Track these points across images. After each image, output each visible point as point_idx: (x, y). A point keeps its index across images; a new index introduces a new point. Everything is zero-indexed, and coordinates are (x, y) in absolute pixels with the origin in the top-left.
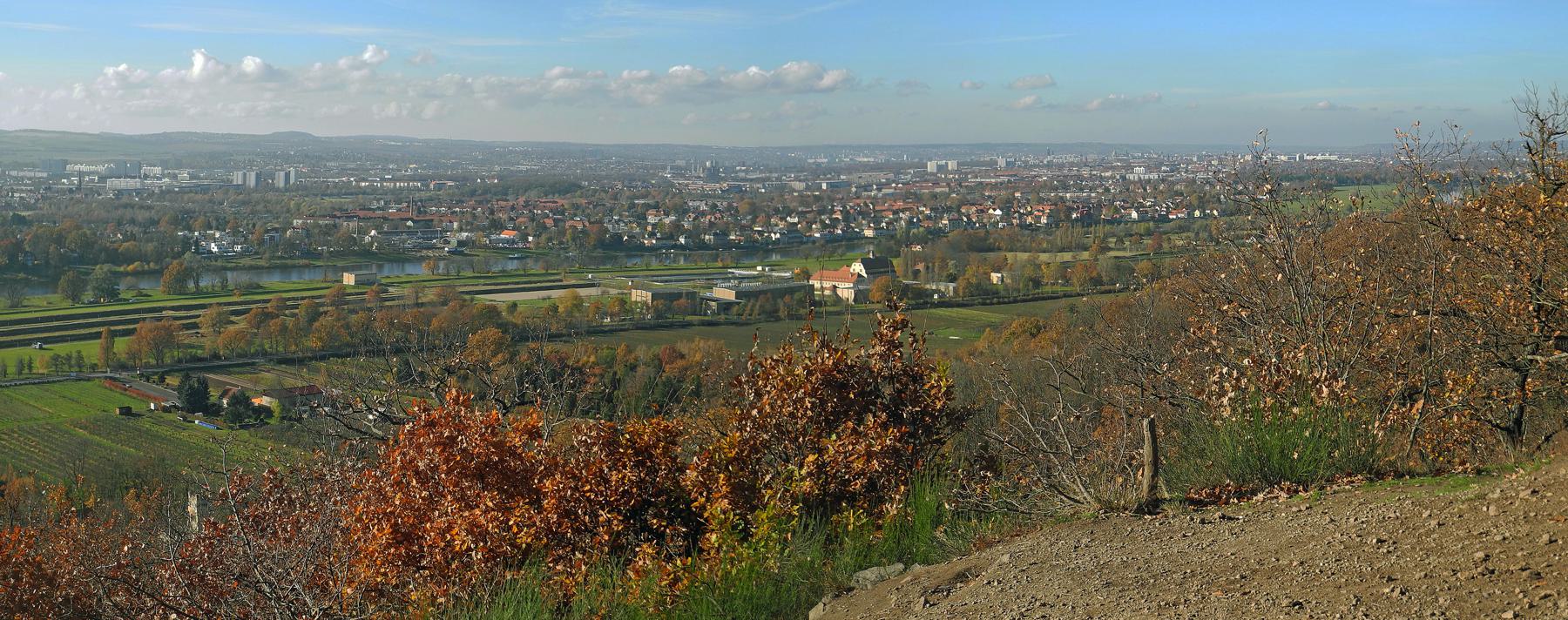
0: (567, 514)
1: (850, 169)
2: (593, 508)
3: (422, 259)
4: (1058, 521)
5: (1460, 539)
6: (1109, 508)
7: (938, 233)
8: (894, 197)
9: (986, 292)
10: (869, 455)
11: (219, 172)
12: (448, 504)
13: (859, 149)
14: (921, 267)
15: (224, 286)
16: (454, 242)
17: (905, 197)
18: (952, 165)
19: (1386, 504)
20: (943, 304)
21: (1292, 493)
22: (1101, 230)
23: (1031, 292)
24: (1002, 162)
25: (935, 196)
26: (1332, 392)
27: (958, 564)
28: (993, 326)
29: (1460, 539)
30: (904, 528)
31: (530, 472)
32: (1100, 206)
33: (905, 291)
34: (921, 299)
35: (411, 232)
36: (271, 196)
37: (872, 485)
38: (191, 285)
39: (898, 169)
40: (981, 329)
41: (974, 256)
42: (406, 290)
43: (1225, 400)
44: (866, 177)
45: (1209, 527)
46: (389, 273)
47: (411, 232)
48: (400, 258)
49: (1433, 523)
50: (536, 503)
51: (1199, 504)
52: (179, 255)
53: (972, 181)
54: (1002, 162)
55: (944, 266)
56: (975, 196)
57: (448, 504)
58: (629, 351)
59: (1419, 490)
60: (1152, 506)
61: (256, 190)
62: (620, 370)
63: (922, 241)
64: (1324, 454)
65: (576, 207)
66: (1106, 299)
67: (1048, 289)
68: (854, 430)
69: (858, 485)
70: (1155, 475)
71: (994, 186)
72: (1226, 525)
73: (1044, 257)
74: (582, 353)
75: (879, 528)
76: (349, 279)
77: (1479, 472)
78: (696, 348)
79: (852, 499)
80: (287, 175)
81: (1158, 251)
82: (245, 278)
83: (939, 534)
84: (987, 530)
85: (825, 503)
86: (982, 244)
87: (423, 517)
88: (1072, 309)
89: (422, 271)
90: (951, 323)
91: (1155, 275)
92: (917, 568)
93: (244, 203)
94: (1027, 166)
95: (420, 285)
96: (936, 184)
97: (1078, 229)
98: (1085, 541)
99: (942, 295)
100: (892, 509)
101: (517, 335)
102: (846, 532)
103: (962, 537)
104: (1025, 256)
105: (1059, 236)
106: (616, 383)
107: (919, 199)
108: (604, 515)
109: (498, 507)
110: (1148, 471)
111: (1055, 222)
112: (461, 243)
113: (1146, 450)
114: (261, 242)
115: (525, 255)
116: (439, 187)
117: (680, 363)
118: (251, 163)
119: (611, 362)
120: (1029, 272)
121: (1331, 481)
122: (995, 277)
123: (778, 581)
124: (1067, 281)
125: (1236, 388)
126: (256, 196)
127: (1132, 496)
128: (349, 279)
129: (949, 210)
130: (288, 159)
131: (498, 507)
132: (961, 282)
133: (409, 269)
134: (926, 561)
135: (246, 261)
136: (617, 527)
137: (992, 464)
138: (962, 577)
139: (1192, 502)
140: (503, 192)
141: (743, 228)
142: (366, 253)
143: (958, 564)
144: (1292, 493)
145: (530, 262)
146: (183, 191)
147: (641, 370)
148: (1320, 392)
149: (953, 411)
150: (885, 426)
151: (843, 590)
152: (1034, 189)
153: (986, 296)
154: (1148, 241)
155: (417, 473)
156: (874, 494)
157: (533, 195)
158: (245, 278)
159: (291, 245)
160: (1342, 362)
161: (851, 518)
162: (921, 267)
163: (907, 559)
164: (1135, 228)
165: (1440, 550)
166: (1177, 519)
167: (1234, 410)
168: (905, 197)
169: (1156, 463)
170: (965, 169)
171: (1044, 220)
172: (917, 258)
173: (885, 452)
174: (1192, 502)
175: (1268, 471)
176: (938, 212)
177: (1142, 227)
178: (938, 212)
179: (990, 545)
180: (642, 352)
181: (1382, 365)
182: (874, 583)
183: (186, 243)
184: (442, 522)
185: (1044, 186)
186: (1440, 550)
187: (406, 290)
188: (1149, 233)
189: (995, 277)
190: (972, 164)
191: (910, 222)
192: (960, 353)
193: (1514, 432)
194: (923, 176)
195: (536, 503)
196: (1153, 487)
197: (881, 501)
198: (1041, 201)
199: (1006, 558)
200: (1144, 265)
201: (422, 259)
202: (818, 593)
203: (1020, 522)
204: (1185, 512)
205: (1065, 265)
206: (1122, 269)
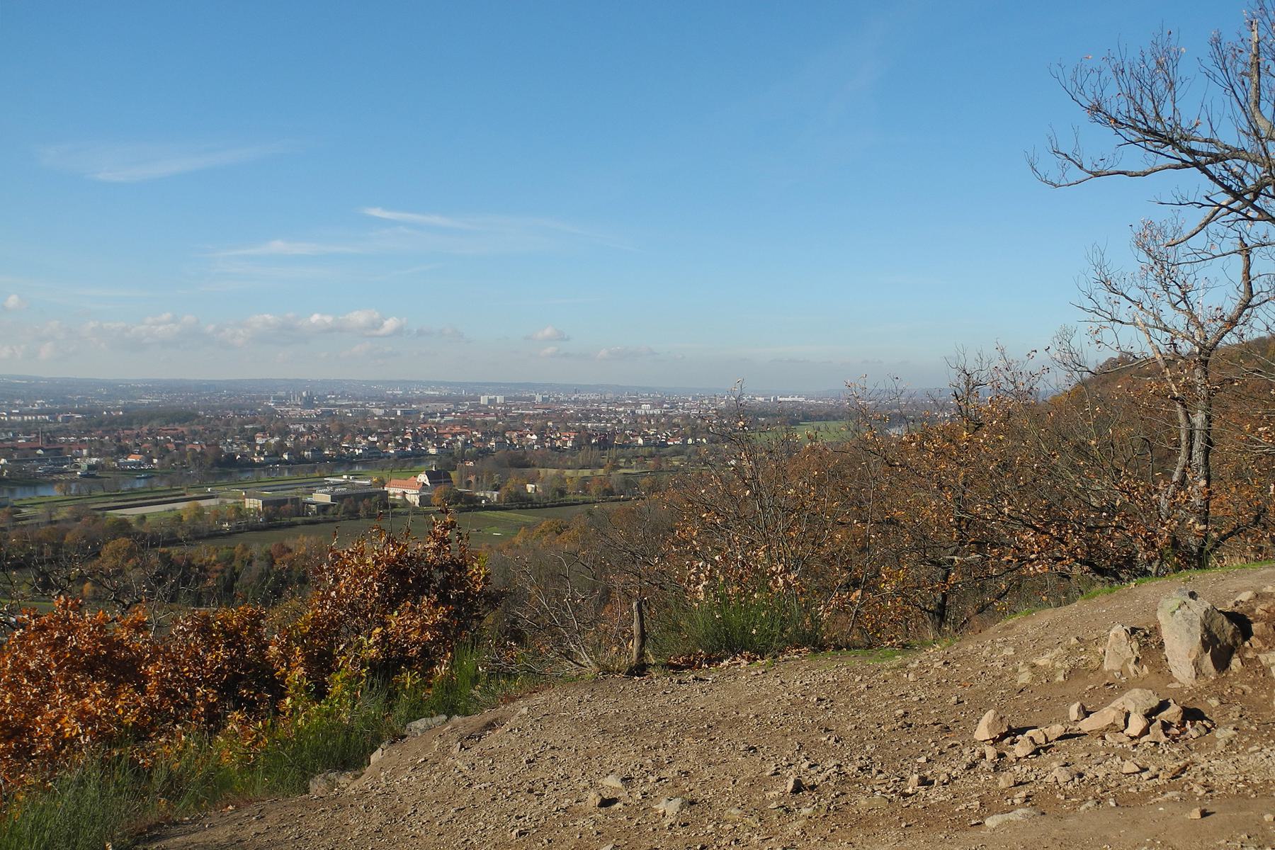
0: (166, 693)
1: (420, 400)
2: (191, 685)
4: (566, 681)
5: (884, 699)
6: (607, 671)
7: (486, 452)
8: (453, 423)
9: (522, 499)
10: (424, 628)
12: (59, 696)
13: (428, 384)
14: (472, 478)
17: (462, 423)
18: (500, 399)
19: (826, 670)
20: (490, 507)
21: (752, 660)
22: (614, 453)
23: (558, 499)
24: (539, 398)
25: (485, 423)
26: (786, 582)
27: (488, 715)
28: (528, 526)
29: (884, 699)
30: (449, 686)
31: (140, 659)
32: (614, 433)
34: (472, 504)
37: (425, 652)
39: (458, 401)
40: (518, 528)
41: (514, 470)
43: (700, 587)
45: (685, 686)
49: (863, 686)
50: (141, 689)
51: (677, 668)
53: (515, 412)
54: (539, 398)
55: (490, 478)
56: (516, 424)
57: (59, 696)
58: (246, 549)
59: (854, 660)
60: (640, 669)
62: (237, 564)
63: (474, 458)
64: (777, 630)
65: (195, 433)
66: (616, 505)
67: (571, 497)
68: (412, 609)
69: (414, 652)
70: (642, 646)
71: (532, 417)
72: (697, 685)
73: (568, 473)
74: (205, 553)
75: (430, 686)
77: (904, 646)
78: (301, 543)
79: (410, 663)
81: (658, 470)
83: (476, 693)
84: (513, 688)
85: (386, 669)
86: (520, 462)
87: (33, 710)
88: (590, 513)
90: (495, 523)
91: (653, 489)
92: (456, 719)
94: (559, 402)
96: (487, 414)
97: (596, 451)
98: (587, 696)
99: (488, 501)
100: (441, 670)
101: (146, 541)
102: (404, 689)
103: (493, 693)
104: (554, 471)
105: (581, 457)
106: (235, 576)
107: (473, 425)
108: (200, 691)
109: (107, 694)
110: (636, 642)
111: (578, 445)
113: (635, 626)
115: (150, 475)
117: (288, 556)
119: (231, 558)
120: (556, 484)
121: (782, 652)
122: (530, 487)
123: (349, 731)
124: (586, 491)
125: (709, 578)
127: (624, 661)
129: (496, 434)
131: (107, 694)
132: (503, 491)
134: (466, 714)
136: (212, 699)
137: (518, 637)
138: (491, 726)
139: (672, 666)
143: (488, 715)
144: (752, 660)
145: (156, 481)
147: (256, 564)
148: (776, 582)
149: (490, 594)
150: (436, 605)
151: (398, 737)
152: (562, 420)
153: (521, 502)
154: (650, 462)
155: (28, 672)
156: (427, 659)
160: (799, 560)
161: (408, 679)
162: (472, 478)
163: (451, 710)
164: (641, 452)
165: (868, 707)
166: (660, 680)
167: (707, 594)
168: (462, 423)
169: (643, 636)
170: (510, 403)
171: (569, 444)
172: (469, 471)
173: (436, 626)
174: (672, 666)
175: (730, 642)
176: (488, 435)
177: (646, 451)
178: (488, 435)
179: (513, 700)
180: (256, 550)
181: (830, 561)
182: (423, 731)
184: (53, 714)
185: (571, 417)
186: (868, 707)
188: (651, 456)
189: (530, 487)
190: (516, 399)
191: (465, 443)
192: (498, 548)
193: (940, 614)
194: (477, 407)
195: (141, 689)
196: (641, 655)
197: (433, 664)
198: (568, 429)
199: (525, 711)
200: (646, 481)
202: (378, 740)
203: (538, 680)
204: (666, 675)
205: (585, 479)
206: (628, 482)
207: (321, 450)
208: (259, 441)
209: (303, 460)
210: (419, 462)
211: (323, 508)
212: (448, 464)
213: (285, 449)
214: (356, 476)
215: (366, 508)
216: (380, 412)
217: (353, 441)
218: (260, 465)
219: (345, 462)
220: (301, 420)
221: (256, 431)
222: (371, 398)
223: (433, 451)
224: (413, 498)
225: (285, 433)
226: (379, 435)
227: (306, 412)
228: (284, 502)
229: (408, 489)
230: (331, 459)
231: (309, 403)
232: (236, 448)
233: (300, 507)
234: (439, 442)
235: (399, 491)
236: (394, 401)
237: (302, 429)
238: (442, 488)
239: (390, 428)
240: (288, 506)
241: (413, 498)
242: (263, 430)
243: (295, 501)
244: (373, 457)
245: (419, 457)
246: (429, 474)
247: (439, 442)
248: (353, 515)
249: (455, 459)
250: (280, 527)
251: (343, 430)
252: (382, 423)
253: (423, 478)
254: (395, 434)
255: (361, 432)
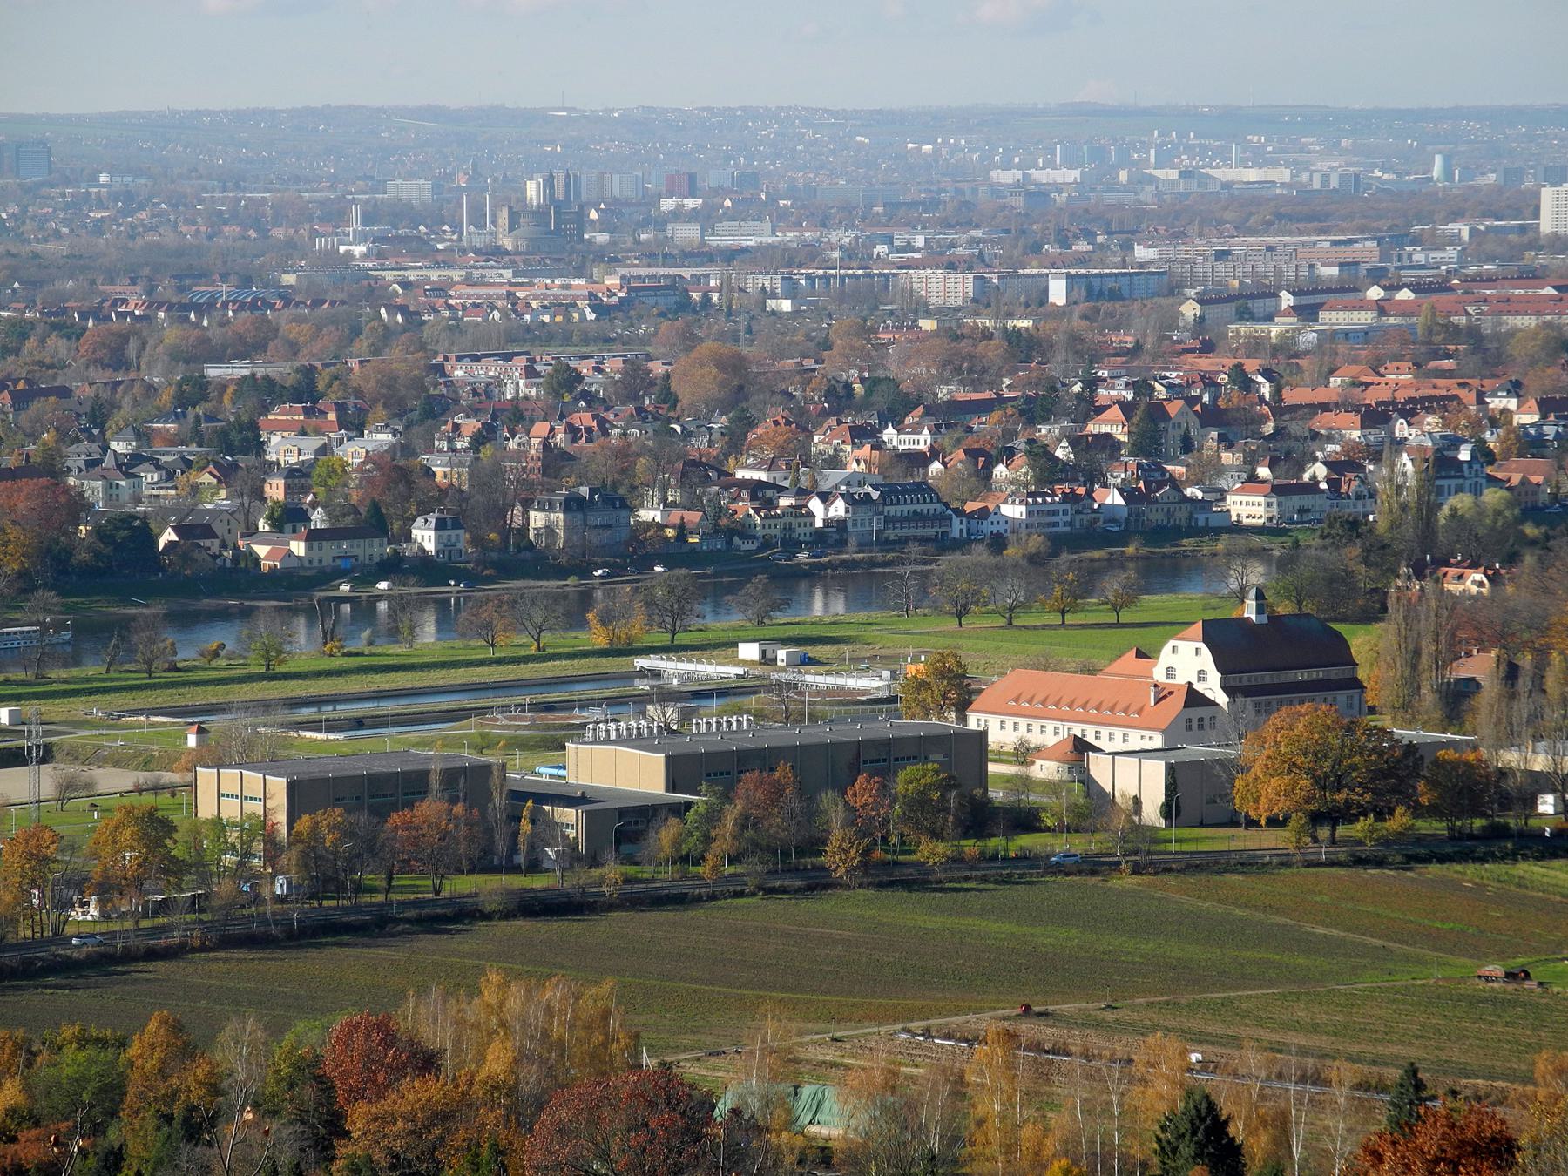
8: (1374, 348)
13: (1230, 126)
14: (1480, 666)
17: (1425, 349)
33: (1398, 773)
39: (1402, 219)
44: (1249, 255)
63: (1495, 548)
107: (1489, 356)
141: (697, 472)
162: (1480, 666)
168: (1425, 349)
172: (1464, 627)
191: (1441, 464)
207: (617, 501)
208: (283, 448)
209: (520, 559)
210: (1164, 571)
211: (625, 825)
212: (1338, 585)
213: (432, 499)
214: (811, 646)
215: (865, 829)
216: (947, 288)
217: (796, 455)
218: (291, 585)
219: (750, 566)
220: (516, 339)
221: (267, 393)
222: (901, 213)
223: (1248, 507)
224: (1136, 778)
225: (423, 407)
226: (947, 416)
227: (538, 293)
228: (411, 785)
229: (1104, 722)
230: (676, 552)
231: (557, 237)
232: (152, 487)
233: (496, 819)
234: (1287, 454)
235: (1049, 734)
236: (1034, 227)
237: (517, 386)
238: (1300, 721)
239: (1015, 380)
240: (430, 808)
241: (1136, 778)
242: (305, 393)
243: (469, 782)
244: (906, 545)
245: (1166, 543)
246: (1227, 642)
247: (1287, 454)
248: (794, 865)
249: (1380, 553)
250: (377, 926)
251: (740, 393)
252: (958, 349)
253: (1188, 662)
254: (1034, 410)
255: (839, 398)
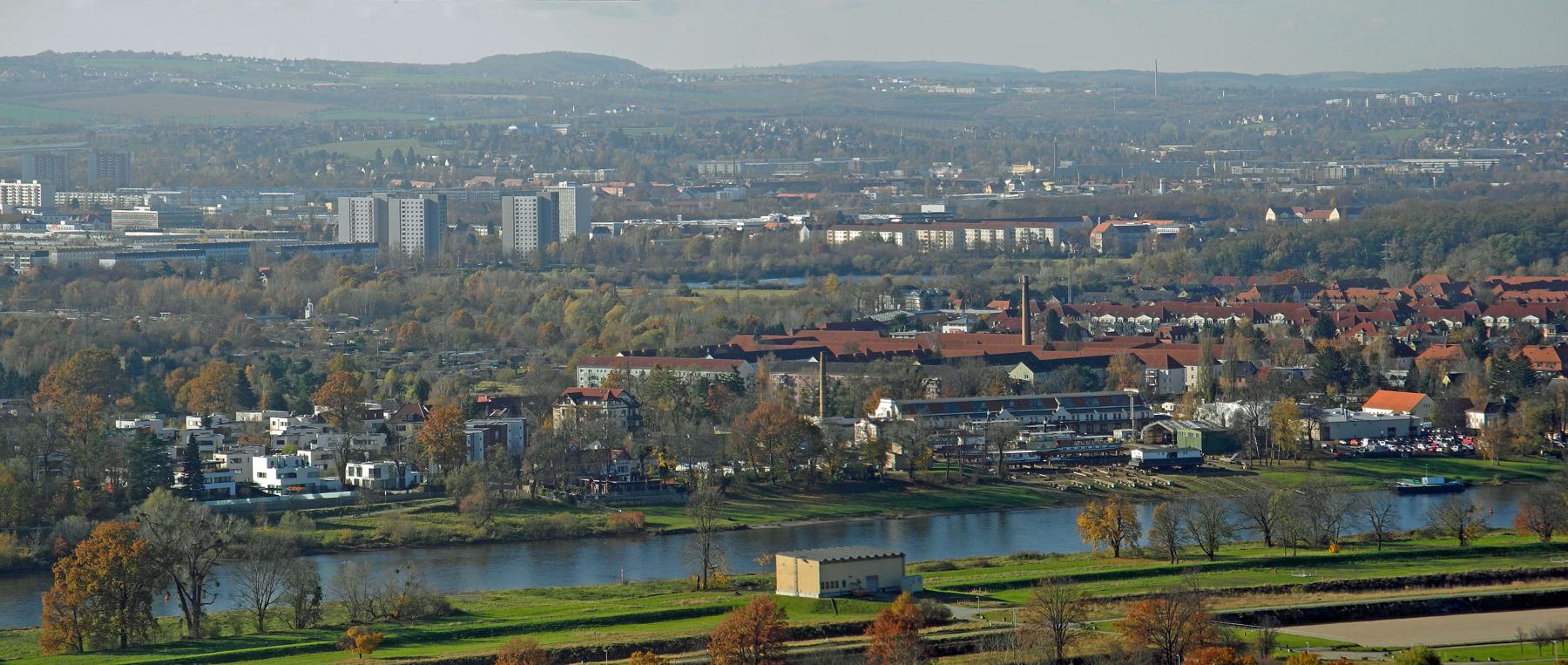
3: (1076, 496)
11: (280, 201)
15: (306, 612)
16: (1189, 438)
35: (1024, 405)
36: (486, 282)
38: (170, 615)
42: (1021, 611)
46: (948, 551)
47: (1024, 405)
48: (986, 494)
52: (121, 503)
61: (426, 263)
76: (798, 578)
80: (548, 210)
82: (389, 582)
89: (1072, 542)
93: (381, 310)
95: (1069, 594)
112: (1217, 441)
114: (454, 452)
116: (1125, 242)
118: (406, 166)
126: (428, 285)
128: (798, 578)
130: (547, 152)
133: (1030, 532)
135: (396, 520)
140: (1365, 253)
142: (862, 483)
146: (133, 265)
157: (1474, 263)
158: (389, 582)
159: (570, 460)
183: (149, 464)
187: (1021, 611)
201: (1076, 496)
